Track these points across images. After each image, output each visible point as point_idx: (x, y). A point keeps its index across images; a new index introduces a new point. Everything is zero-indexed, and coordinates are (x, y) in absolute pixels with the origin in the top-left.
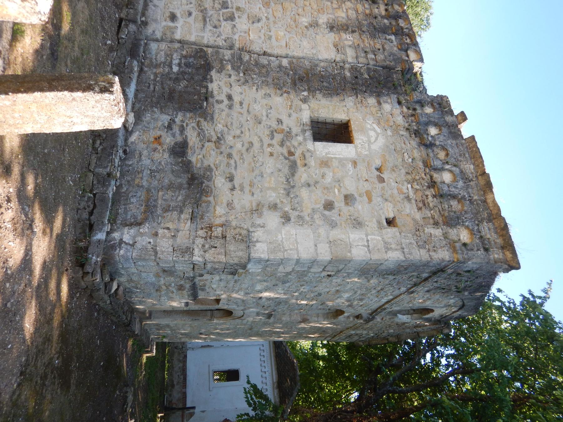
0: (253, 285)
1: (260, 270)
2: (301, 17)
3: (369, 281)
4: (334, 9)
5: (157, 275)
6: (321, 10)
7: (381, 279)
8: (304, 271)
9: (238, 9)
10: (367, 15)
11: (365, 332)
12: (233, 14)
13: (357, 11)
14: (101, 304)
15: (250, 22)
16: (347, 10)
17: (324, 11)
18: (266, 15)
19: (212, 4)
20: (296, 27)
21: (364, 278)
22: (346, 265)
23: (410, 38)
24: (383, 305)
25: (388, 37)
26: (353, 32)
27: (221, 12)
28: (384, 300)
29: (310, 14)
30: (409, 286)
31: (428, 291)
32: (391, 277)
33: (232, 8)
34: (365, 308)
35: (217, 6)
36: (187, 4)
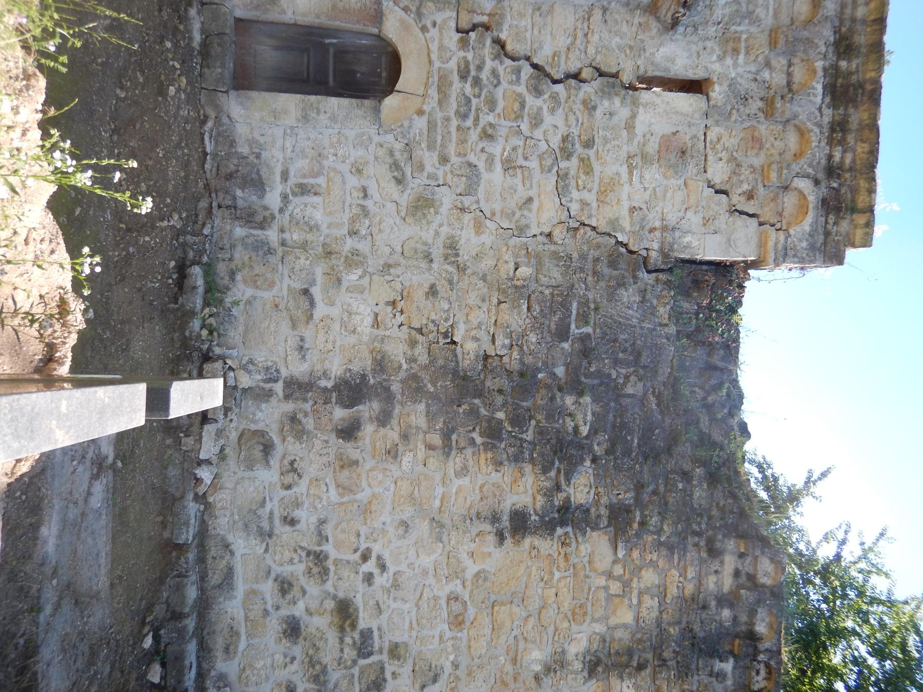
2: (530, 645)
4: (610, 597)
6: (578, 614)
9: (395, 651)
10: (686, 601)
12: (382, 669)
13: (662, 593)
15: (417, 686)
16: (640, 593)
17: (585, 614)
18: (452, 657)
19: (337, 655)
20: (515, 679)
23: (767, 666)
25: (719, 665)
26: (641, 667)
27: (356, 671)
29: (551, 630)
33: (381, 651)
35: (350, 653)
36: (286, 665)
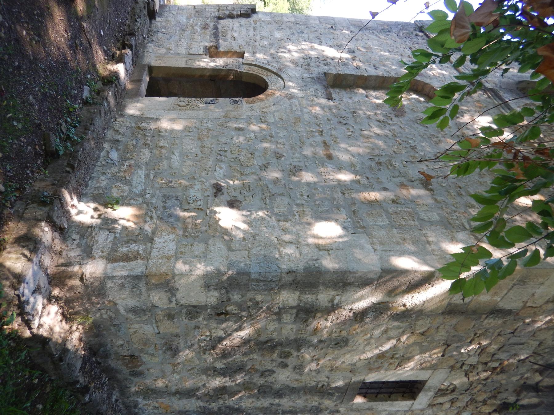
5: (188, 18)
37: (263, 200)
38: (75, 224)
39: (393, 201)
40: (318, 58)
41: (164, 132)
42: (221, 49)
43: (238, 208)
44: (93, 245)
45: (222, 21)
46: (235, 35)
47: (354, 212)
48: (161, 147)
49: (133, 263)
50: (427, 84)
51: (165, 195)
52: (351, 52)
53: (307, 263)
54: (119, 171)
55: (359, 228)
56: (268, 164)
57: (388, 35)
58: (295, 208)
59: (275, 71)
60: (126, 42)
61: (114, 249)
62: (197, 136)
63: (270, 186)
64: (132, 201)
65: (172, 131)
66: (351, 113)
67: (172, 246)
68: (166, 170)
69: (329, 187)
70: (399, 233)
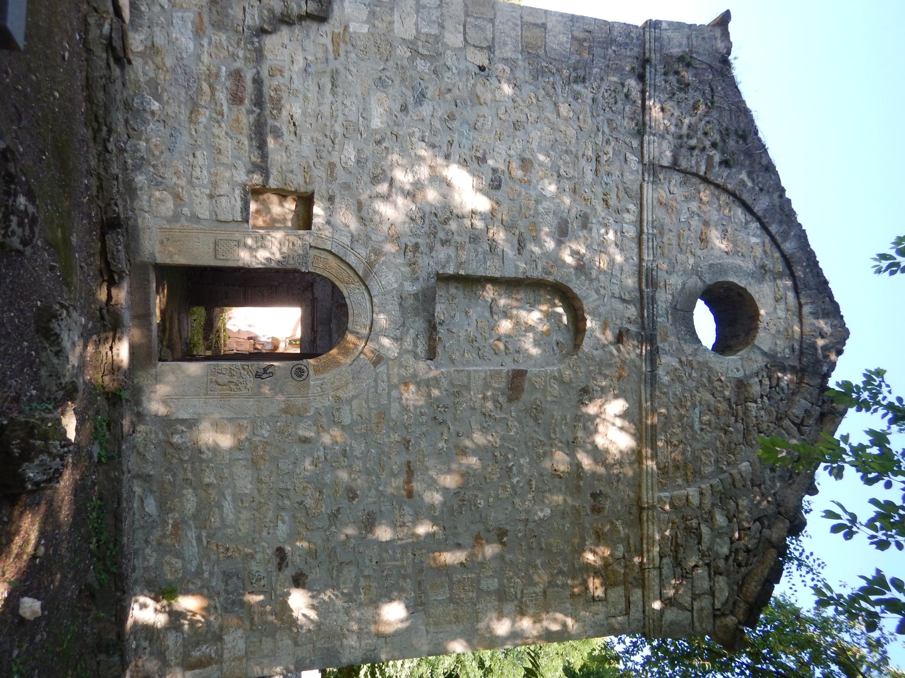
0: (365, 114)
1: (365, 29)
3: (555, 104)
5: (199, 32)
7: (576, 106)
8: (437, 38)
11: (693, 492)
14: (94, 33)
21: (543, 92)
22: (492, 21)
24: (641, 259)
28: (631, 232)
30: (635, 144)
31: (674, 166)
32: (586, 92)
34: (617, 295)
37: (330, 571)
38: (138, 628)
39: (462, 563)
40: (436, 215)
41: (207, 451)
42: (273, 184)
43: (303, 587)
44: (165, 651)
45: (270, 41)
46: (297, 111)
47: (420, 583)
48: (208, 485)
49: (209, 669)
50: (579, 300)
51: (224, 572)
52: (494, 185)
53: (365, 654)
54: (164, 536)
55: (420, 605)
56: (338, 510)
57: (577, 96)
58: (362, 583)
59: (360, 273)
60: (113, 269)
61: (186, 654)
62: (249, 457)
63: (338, 550)
64: (191, 586)
65: (215, 449)
66: (453, 394)
67: (241, 644)
68: (219, 528)
69: (400, 546)
70: (454, 609)
